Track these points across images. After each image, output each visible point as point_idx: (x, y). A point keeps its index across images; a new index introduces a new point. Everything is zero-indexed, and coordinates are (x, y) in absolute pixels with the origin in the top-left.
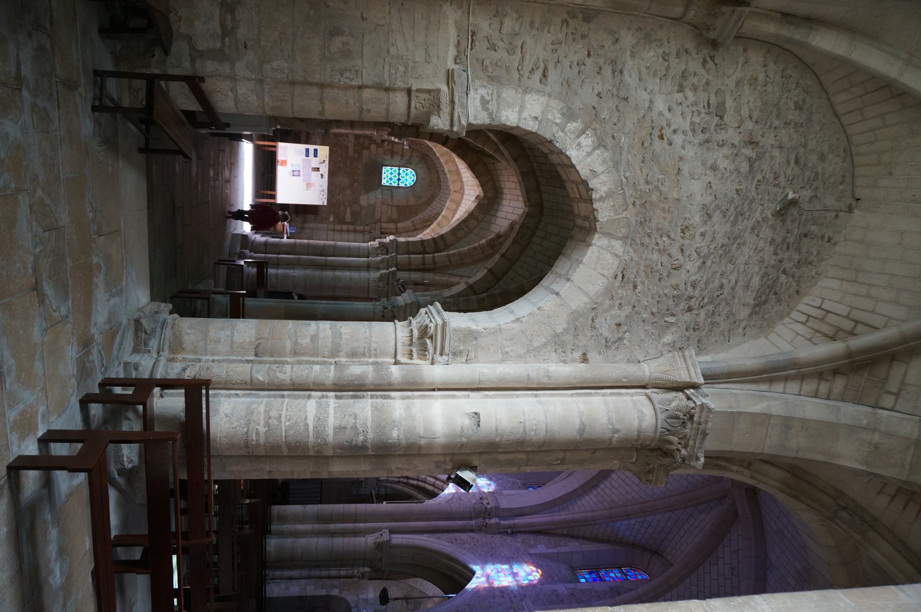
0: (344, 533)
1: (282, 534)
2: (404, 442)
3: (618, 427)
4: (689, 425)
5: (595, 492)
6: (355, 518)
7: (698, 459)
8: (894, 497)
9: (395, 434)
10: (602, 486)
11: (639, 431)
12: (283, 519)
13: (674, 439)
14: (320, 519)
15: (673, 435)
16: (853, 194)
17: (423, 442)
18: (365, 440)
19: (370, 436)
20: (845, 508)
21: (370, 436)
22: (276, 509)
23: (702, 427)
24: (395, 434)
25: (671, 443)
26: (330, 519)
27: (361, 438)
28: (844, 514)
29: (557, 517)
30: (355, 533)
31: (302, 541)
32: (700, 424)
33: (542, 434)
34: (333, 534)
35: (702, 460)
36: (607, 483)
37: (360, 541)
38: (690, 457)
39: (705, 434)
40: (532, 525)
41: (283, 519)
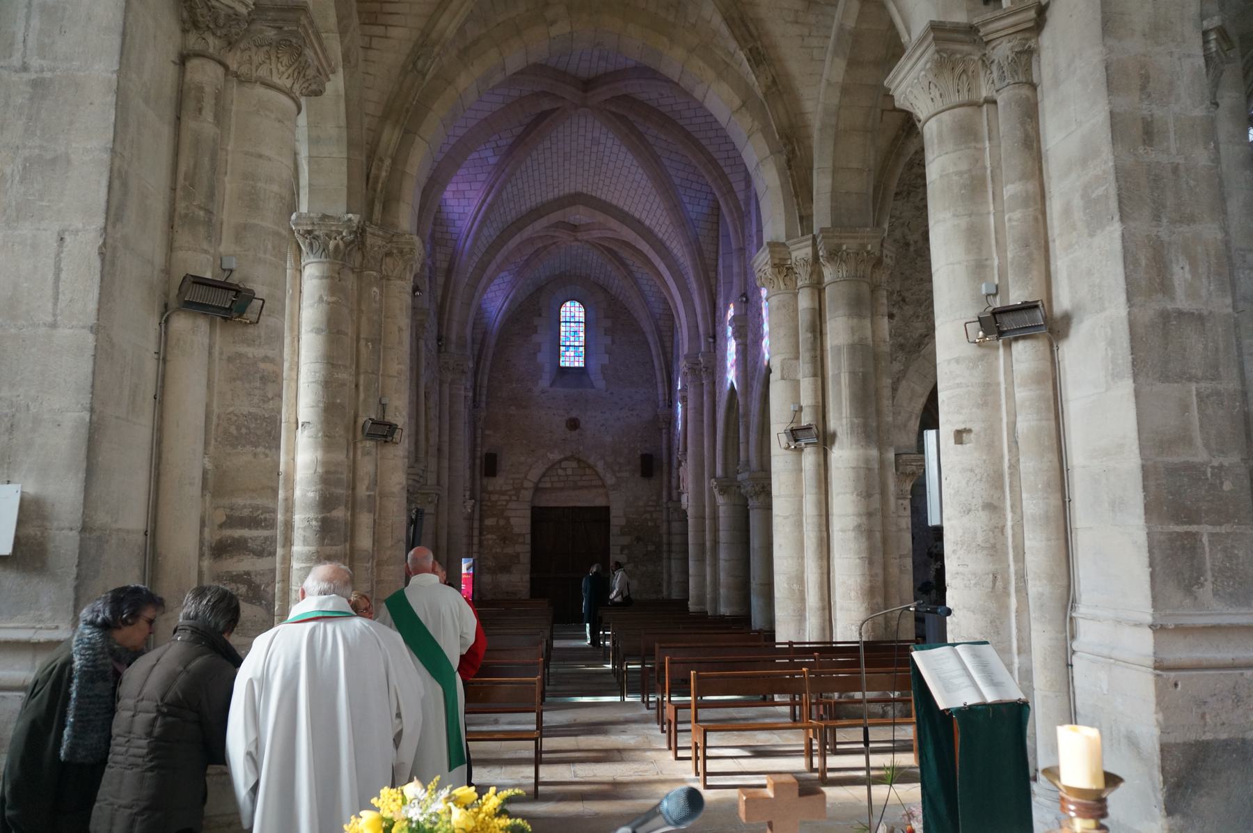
0: (716, 531)
1: (715, 600)
2: (319, 487)
3: (316, 297)
4: (316, 233)
5: (668, 243)
6: (701, 518)
7: (350, 220)
8: (386, 26)
9: (311, 494)
10: (660, 235)
11: (322, 277)
12: (701, 599)
13: (332, 244)
14: (701, 560)
15: (327, 246)
16: (199, 55)
17: (320, 470)
18: (316, 519)
19: (312, 515)
20: (415, 64)
21: (312, 515)
22: (692, 607)
23: (316, 221)
24: (311, 494)
25: (337, 246)
26: (701, 546)
27: (314, 523)
28: (420, 63)
29: (694, 285)
30: (715, 518)
31: (723, 576)
32: (313, 224)
33: (318, 366)
34: (716, 542)
35: (350, 215)
36: (656, 230)
37: (723, 511)
38: (348, 227)
39: (324, 217)
40: (704, 315)
41: (701, 599)
